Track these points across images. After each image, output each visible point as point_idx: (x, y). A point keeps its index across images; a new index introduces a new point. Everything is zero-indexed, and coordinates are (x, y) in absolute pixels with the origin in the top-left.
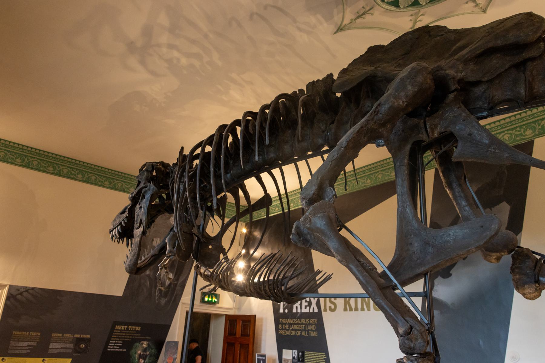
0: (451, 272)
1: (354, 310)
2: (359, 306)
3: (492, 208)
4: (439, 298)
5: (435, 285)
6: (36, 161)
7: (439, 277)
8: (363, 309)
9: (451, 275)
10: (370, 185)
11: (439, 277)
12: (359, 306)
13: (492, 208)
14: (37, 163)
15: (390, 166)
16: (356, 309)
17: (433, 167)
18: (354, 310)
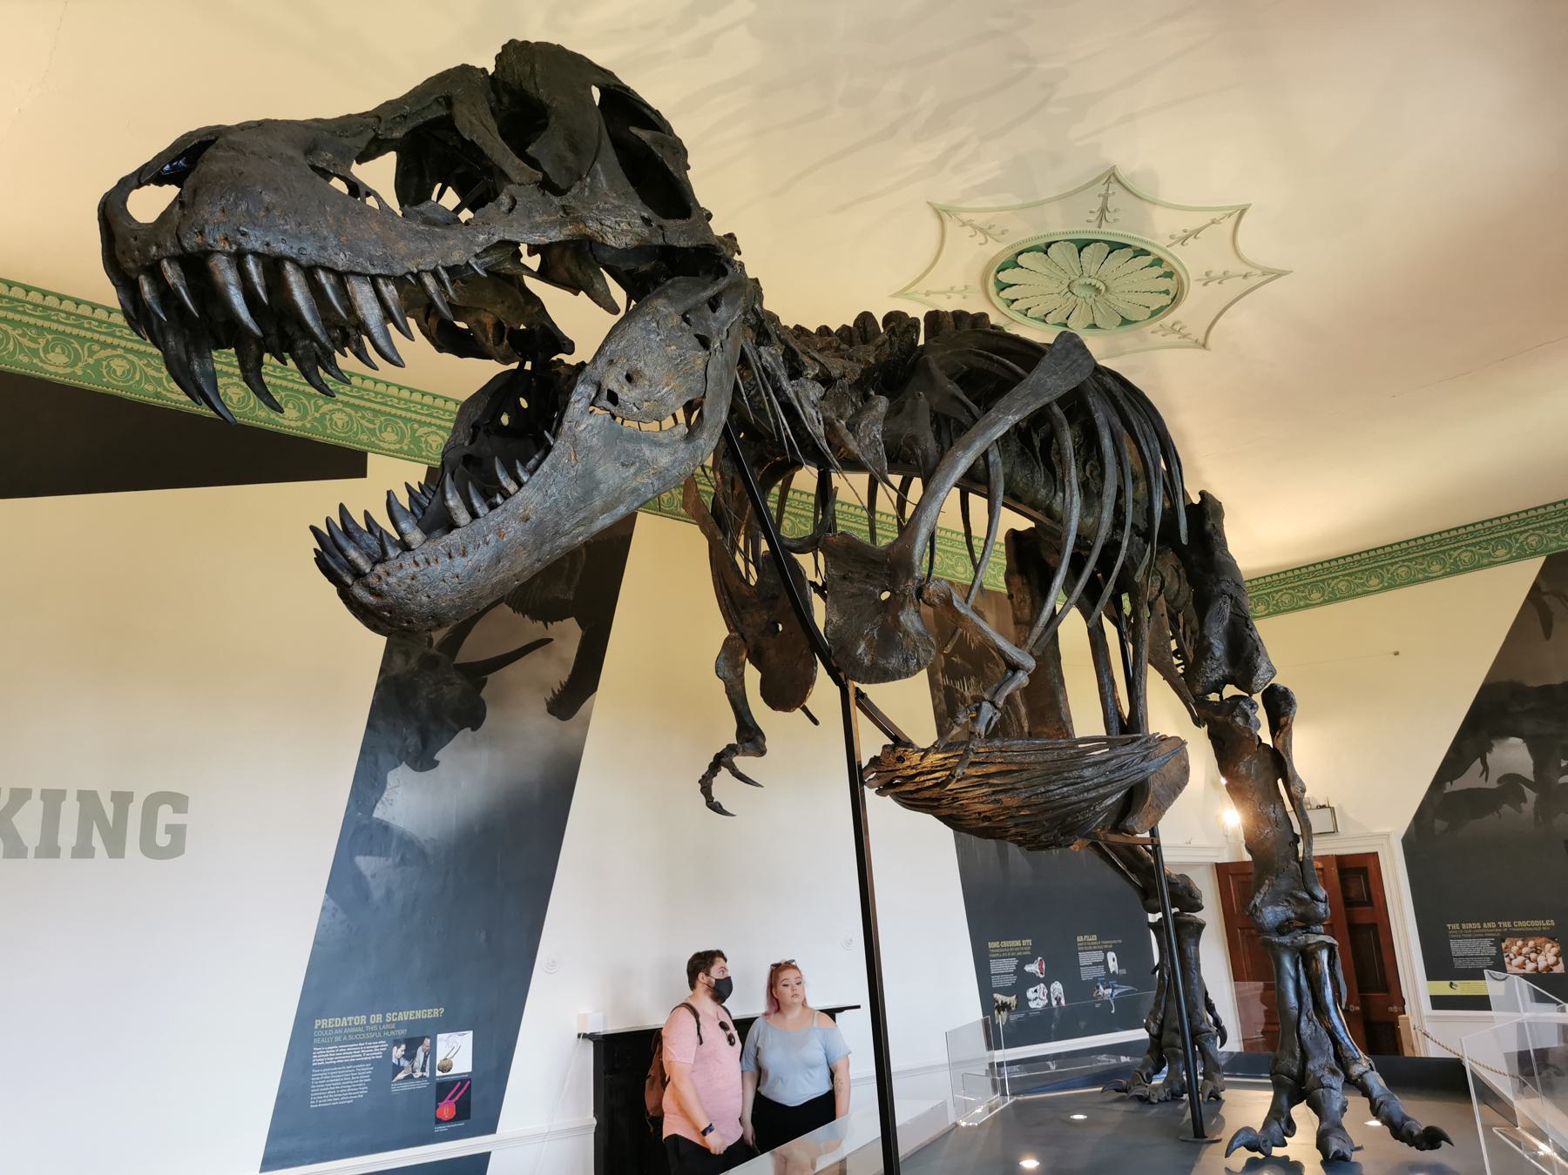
0: (436, 758)
1: (31, 853)
2: (67, 837)
3: (549, 624)
4: (393, 822)
5: (388, 787)
6: (1533, 534)
7: (404, 763)
8: (83, 850)
9: (435, 764)
10: (65, 376)
11: (404, 763)
12: (67, 837)
13: (549, 624)
14: (1537, 538)
15: (285, 383)
16: (49, 849)
17: (426, 460)
18: (31, 853)
